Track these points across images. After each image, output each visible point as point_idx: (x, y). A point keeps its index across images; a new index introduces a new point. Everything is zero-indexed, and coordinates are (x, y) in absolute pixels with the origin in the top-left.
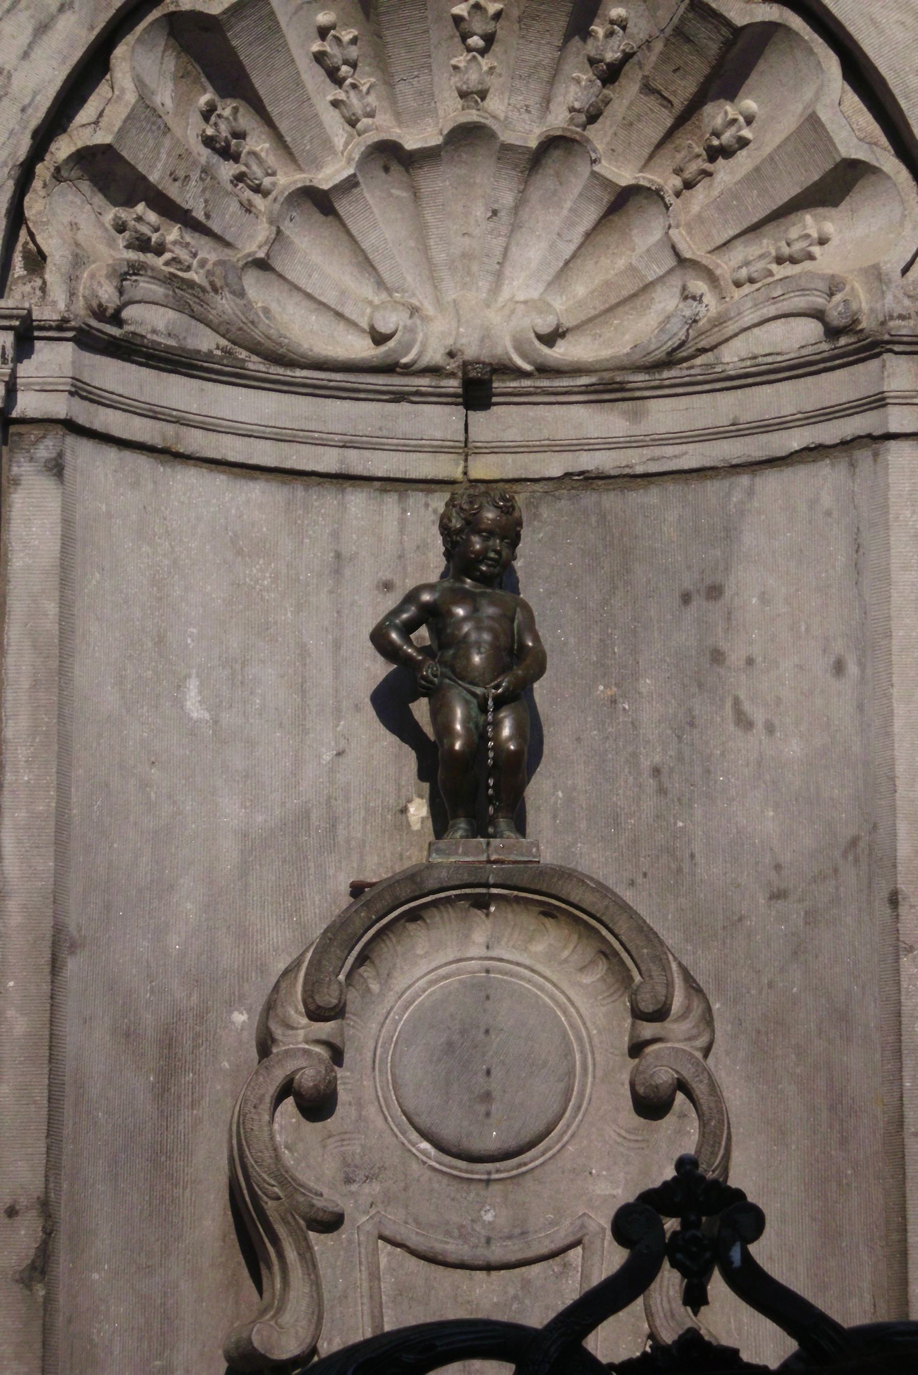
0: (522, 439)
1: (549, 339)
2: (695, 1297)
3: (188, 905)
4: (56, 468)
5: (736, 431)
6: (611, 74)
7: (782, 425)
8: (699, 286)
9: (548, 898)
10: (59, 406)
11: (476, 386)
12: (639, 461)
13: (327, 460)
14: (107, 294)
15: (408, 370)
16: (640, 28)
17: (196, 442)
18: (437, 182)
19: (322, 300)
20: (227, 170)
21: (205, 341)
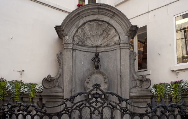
0: (99, 50)
6: (104, 31)
7: (112, 49)
9: (101, 73)
10: (75, 48)
13: (89, 51)
14: (78, 42)
16: (105, 29)
20: (84, 36)
21: (83, 45)
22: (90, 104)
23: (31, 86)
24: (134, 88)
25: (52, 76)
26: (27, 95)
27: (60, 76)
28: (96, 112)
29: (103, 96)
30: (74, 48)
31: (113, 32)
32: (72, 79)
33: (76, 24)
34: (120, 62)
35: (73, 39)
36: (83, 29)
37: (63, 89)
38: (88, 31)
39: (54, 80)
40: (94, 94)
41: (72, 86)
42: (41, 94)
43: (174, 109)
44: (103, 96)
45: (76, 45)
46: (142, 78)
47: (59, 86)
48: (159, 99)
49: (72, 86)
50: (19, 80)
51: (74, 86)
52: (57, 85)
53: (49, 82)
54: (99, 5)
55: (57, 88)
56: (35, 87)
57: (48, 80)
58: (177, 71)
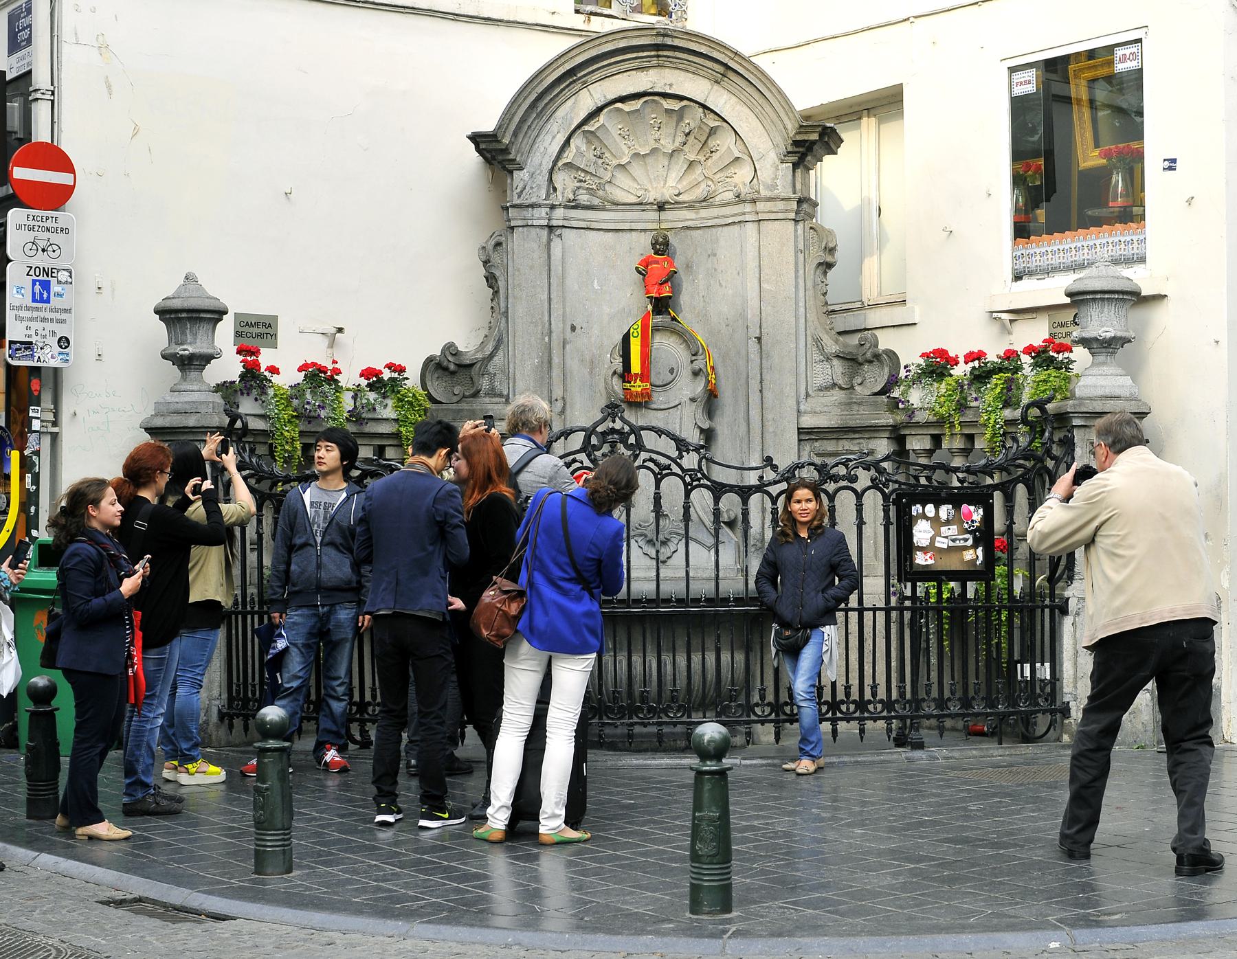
0: (672, 218)
1: (679, 194)
2: (614, 422)
3: (596, 331)
4: (560, 236)
5: (718, 217)
6: (688, 135)
8: (710, 183)
11: (661, 207)
12: (698, 224)
13: (627, 226)
14: (571, 197)
15: (646, 204)
16: (692, 125)
17: (594, 225)
18: (649, 160)
19: (624, 189)
20: (600, 161)
21: (596, 202)
24: (822, 394)
27: (496, 348)
29: (632, 440)
30: (554, 223)
31: (725, 142)
32: (550, 362)
33: (560, 113)
34: (757, 285)
35: (550, 180)
36: (592, 132)
38: (619, 139)
39: (472, 365)
40: (604, 433)
44: (632, 440)
45: (565, 207)
46: (855, 351)
47: (493, 393)
53: (453, 373)
54: (658, 35)
57: (446, 369)
58: (1005, 316)
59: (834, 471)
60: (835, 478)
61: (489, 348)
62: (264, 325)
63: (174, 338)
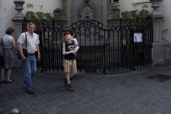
22: (84, 26)
23: (48, 15)
25: (59, 8)
26: (46, 20)
27: (64, 8)
28: (87, 29)
29: (91, 22)
37: (67, 17)
40: (86, 21)
41: (72, 15)
42: (54, 20)
43: (126, 27)
44: (91, 22)
47: (64, 15)
48: (124, 21)
49: (72, 15)
50: (41, 12)
51: (73, 15)
52: (63, 13)
53: (58, 12)
55: (63, 16)
56: (50, 16)
57: (57, 11)
59: (123, 27)
60: (123, 28)
61: (64, 8)
62: (31, 5)
63: (16, 7)
